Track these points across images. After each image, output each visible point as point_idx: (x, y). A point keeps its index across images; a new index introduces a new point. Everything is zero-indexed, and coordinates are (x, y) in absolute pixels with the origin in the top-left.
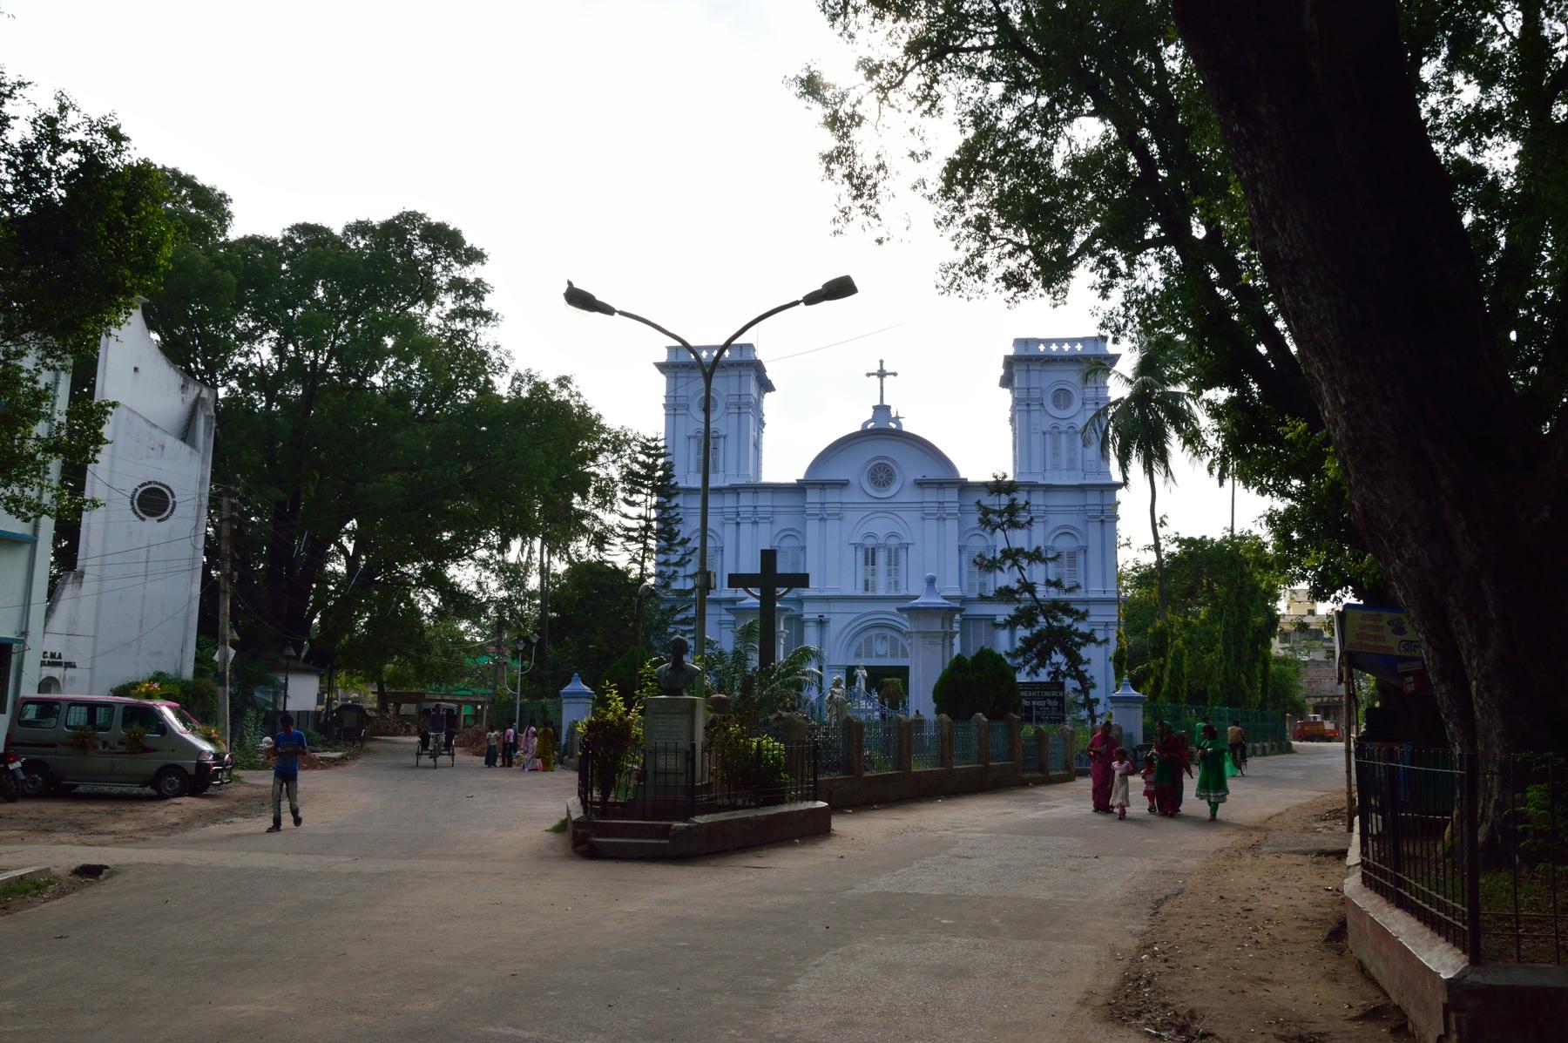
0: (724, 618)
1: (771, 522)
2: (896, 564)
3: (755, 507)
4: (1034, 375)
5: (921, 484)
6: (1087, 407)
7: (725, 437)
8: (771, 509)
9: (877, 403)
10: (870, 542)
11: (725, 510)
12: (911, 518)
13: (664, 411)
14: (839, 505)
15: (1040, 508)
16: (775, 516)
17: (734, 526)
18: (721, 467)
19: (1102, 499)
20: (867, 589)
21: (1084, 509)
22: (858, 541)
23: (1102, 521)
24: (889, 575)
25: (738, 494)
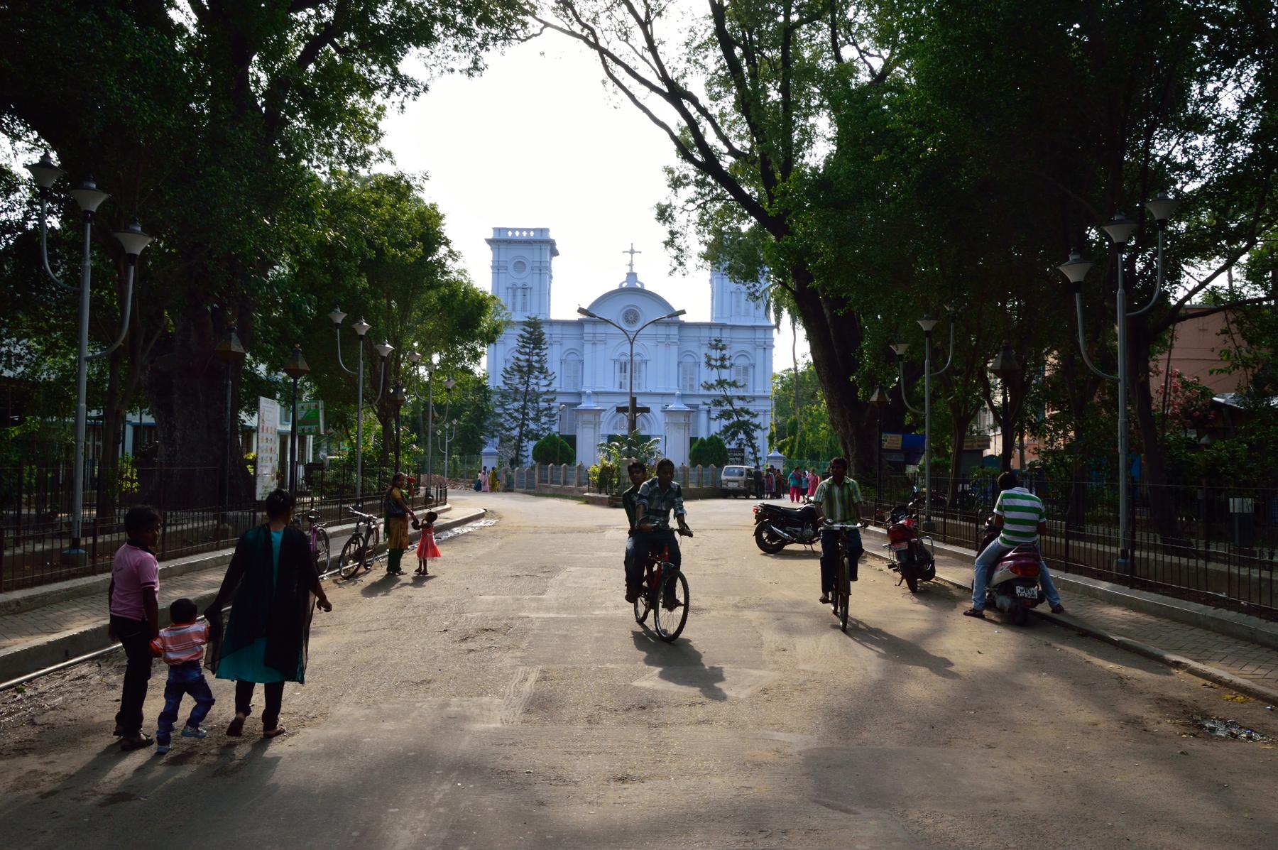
1: (561, 344)
2: (639, 372)
7: (531, 288)
9: (628, 271)
18: (528, 308)
19: (765, 335)
20: (621, 388)
21: (754, 341)
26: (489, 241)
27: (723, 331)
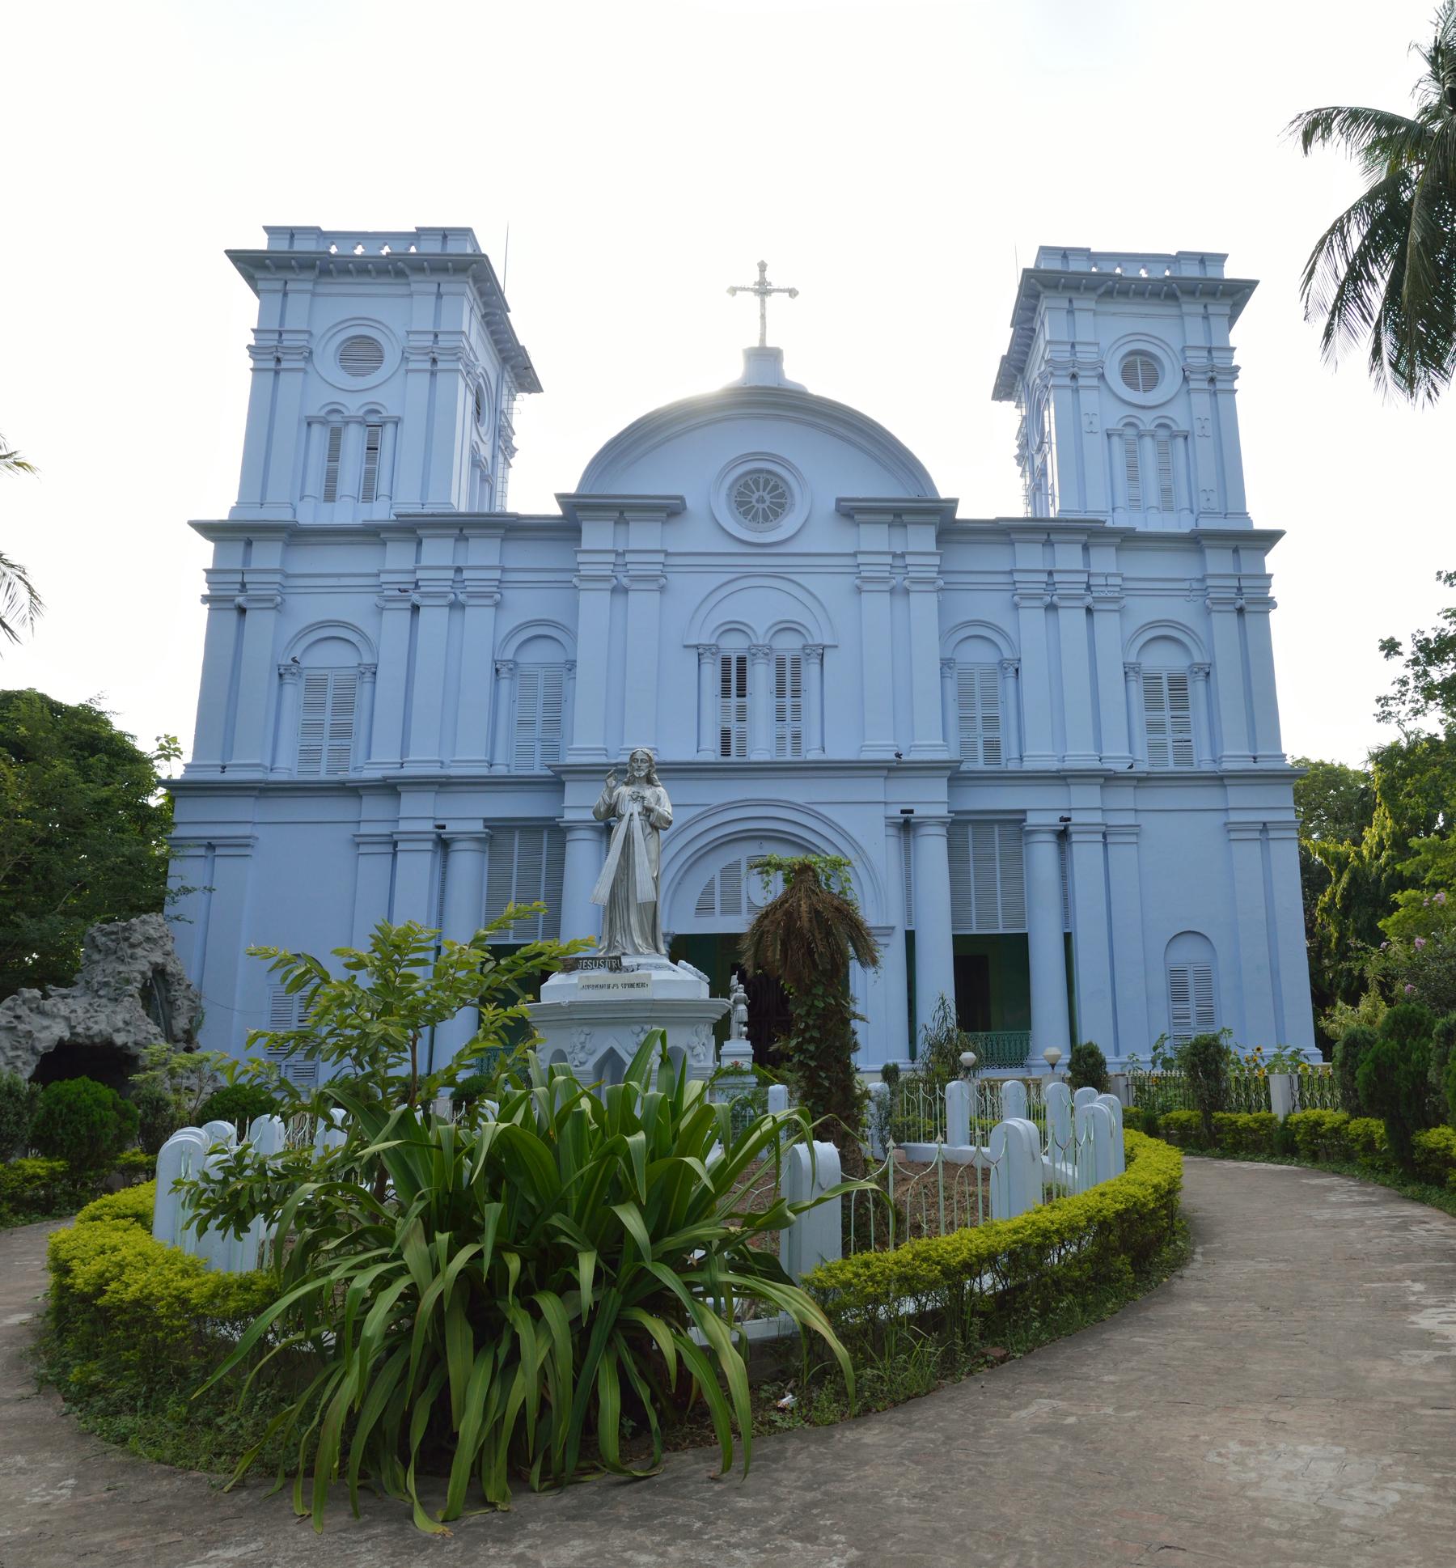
0: (365, 829)
1: (497, 605)
2: (796, 694)
3: (459, 570)
4: (1084, 320)
5: (851, 512)
6: (1193, 385)
7: (397, 422)
8: (497, 574)
10: (734, 645)
11: (384, 578)
12: (831, 588)
13: (251, 363)
14: (661, 558)
15: (1111, 581)
16: (506, 592)
17: (408, 614)
20: (726, 751)
21: (1201, 587)
22: (705, 640)
23: (1240, 611)
24: (781, 718)
25: (420, 543)
26: (248, 263)
27: (1094, 553)
